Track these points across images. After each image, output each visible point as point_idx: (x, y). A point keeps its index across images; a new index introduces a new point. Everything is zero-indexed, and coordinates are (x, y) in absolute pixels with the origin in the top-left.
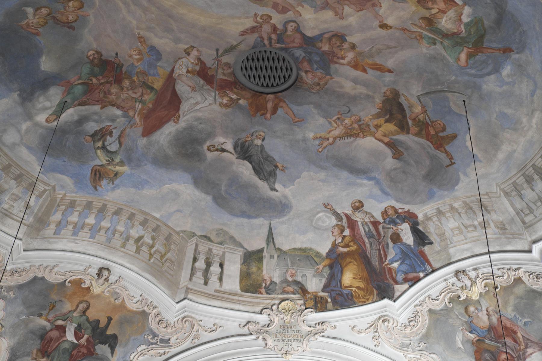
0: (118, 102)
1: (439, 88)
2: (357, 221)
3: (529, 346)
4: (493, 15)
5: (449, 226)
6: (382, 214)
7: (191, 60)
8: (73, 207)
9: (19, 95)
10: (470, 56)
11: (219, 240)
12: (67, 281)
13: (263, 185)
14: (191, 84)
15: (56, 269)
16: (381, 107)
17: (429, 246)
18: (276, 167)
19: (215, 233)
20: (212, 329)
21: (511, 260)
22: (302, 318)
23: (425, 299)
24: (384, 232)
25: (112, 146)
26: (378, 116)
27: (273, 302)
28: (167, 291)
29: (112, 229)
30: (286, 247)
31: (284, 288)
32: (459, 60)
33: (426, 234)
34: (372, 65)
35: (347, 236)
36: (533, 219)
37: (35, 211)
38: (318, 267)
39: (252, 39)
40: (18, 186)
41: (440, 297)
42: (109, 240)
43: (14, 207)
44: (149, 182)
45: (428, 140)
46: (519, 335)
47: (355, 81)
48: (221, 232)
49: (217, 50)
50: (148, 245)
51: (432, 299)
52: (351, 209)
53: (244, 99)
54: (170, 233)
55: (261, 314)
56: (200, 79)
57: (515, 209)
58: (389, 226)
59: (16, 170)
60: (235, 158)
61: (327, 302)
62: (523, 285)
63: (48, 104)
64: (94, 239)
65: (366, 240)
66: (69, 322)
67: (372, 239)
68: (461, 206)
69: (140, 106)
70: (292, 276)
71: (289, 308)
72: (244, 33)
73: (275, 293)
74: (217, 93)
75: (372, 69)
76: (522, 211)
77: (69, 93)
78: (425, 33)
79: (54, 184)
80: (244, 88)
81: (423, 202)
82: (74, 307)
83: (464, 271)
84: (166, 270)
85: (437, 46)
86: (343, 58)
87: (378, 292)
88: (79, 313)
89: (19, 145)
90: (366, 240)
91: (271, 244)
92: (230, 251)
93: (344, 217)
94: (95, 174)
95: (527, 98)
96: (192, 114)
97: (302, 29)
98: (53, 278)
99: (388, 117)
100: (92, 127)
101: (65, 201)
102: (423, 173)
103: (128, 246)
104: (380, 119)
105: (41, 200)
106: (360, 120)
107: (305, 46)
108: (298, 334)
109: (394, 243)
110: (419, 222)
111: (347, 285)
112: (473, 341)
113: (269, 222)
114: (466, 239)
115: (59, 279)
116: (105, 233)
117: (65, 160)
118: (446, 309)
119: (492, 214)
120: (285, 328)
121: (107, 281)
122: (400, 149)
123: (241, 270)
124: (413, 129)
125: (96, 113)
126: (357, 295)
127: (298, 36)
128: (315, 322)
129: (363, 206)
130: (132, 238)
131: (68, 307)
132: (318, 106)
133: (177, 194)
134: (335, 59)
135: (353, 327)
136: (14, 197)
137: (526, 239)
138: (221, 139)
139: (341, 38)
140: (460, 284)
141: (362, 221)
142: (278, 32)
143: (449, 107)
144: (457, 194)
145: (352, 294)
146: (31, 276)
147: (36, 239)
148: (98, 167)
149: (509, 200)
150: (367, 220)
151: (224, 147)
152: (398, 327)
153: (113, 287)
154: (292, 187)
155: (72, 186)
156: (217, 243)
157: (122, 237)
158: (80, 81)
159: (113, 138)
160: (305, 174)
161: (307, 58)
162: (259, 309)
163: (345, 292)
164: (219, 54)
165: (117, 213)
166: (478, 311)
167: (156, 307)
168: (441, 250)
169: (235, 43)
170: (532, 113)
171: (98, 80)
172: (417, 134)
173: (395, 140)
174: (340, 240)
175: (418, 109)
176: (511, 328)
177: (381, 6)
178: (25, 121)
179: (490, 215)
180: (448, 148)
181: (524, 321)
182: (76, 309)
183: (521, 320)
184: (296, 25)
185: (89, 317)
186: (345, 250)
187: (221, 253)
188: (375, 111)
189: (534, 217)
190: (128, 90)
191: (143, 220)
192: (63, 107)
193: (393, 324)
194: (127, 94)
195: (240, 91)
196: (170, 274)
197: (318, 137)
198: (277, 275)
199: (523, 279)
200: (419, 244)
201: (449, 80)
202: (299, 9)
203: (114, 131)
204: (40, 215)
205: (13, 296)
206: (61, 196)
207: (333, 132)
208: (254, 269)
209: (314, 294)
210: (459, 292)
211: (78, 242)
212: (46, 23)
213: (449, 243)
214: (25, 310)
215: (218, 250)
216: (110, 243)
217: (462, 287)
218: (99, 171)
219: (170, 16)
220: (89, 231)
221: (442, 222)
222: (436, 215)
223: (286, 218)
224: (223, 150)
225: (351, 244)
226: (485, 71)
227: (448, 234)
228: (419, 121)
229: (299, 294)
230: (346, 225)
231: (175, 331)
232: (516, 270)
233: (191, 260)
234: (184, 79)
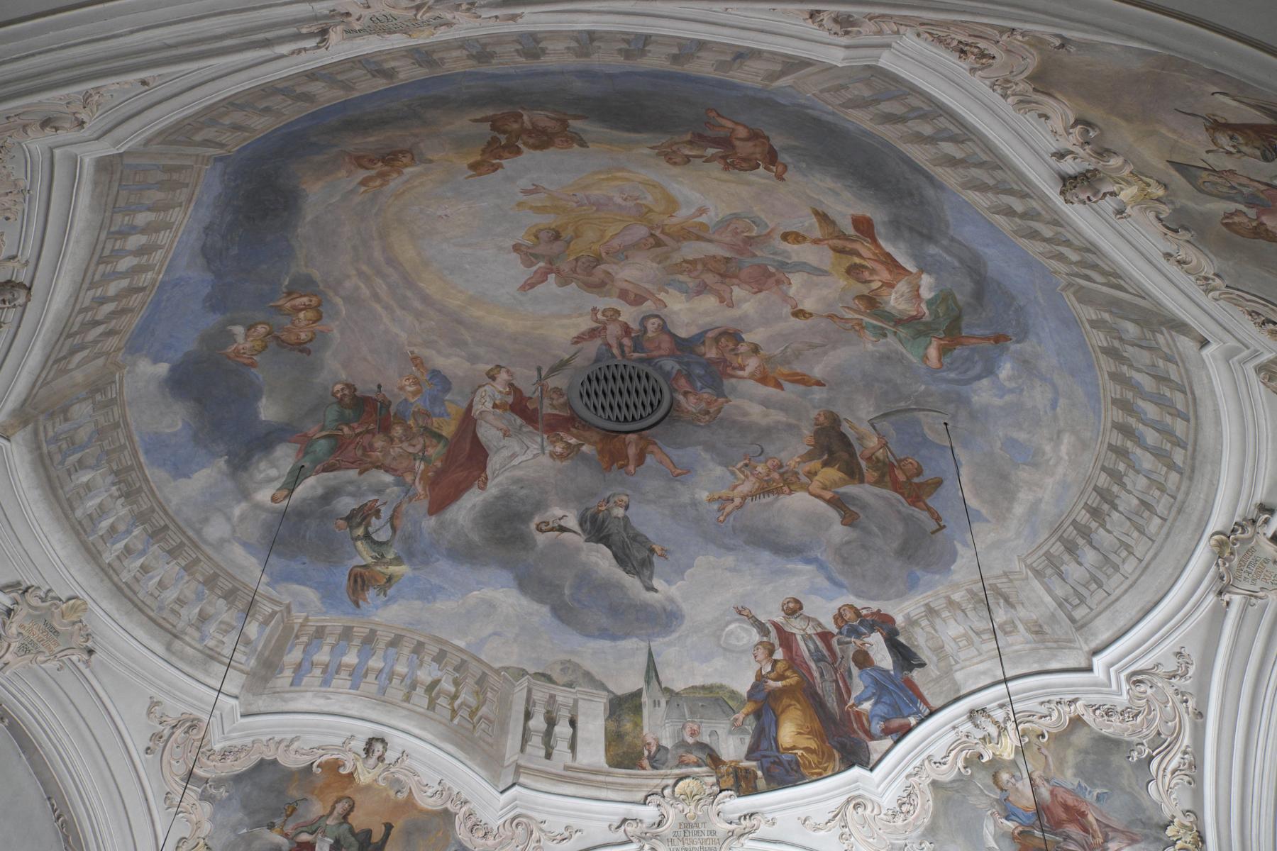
0: (388, 461)
1: (902, 404)
2: (795, 634)
3: (1110, 837)
4: (969, 286)
5: (950, 634)
6: (835, 619)
7: (500, 385)
8: (322, 638)
9: (228, 462)
10: (943, 351)
11: (566, 679)
12: (315, 765)
13: (632, 583)
14: (501, 426)
15: (295, 745)
16: (813, 443)
17: (919, 669)
18: (652, 551)
19: (558, 668)
20: (563, 837)
21: (1061, 686)
22: (715, 808)
23: (922, 764)
24: (840, 649)
25: (381, 533)
26: (809, 457)
27: (665, 782)
28: (483, 773)
29: (386, 670)
30: (678, 686)
31: (681, 756)
32: (927, 358)
33: (913, 649)
34: (788, 375)
35: (779, 661)
36: (1087, 614)
37: (259, 649)
38: (736, 716)
39: (592, 347)
40: (230, 608)
41: (948, 758)
42: (383, 690)
43: (224, 643)
44: (444, 588)
45: (896, 491)
46: (1091, 818)
47: (766, 403)
48: (567, 666)
49: (539, 370)
50: (447, 694)
51: (935, 763)
52: (783, 614)
53: (590, 443)
54: (484, 673)
55: (645, 804)
56: (516, 417)
57: (1055, 598)
58: (848, 639)
59: (227, 583)
60: (582, 540)
61: (756, 777)
62: (1085, 730)
63: (273, 472)
64: (357, 689)
65: (813, 665)
66: (320, 836)
67: (823, 663)
68: (965, 598)
69: (422, 467)
70: (693, 734)
71: (692, 792)
72: (578, 340)
73: (667, 767)
74: (545, 436)
75: (793, 382)
76: (1066, 600)
77: (306, 454)
78: (867, 319)
79: (288, 602)
80: (587, 426)
81: (901, 595)
82: (329, 809)
83: (983, 710)
84: (480, 738)
85: (888, 340)
86: (742, 368)
87: (842, 755)
88: (337, 819)
89: (229, 541)
90: (813, 665)
91: (654, 681)
92: (586, 698)
93: (771, 628)
94: (356, 581)
95: (1046, 412)
96: (507, 474)
97: (669, 326)
98: (292, 761)
99: (826, 457)
100: (346, 504)
101: (307, 628)
102: (895, 545)
103: (415, 699)
104: (813, 463)
105: (268, 630)
106: (781, 466)
107: (678, 353)
108: (710, 837)
109: (860, 668)
110: (899, 628)
111: (788, 746)
112: (1013, 833)
113: (647, 644)
114: (980, 654)
115: (303, 761)
116: (376, 678)
117: (306, 560)
118: (960, 779)
119: (1018, 608)
120: (687, 827)
121: (383, 761)
122: (852, 508)
123: (606, 729)
124: (870, 475)
125: (351, 482)
126: (807, 762)
127: (665, 338)
128: (737, 815)
129: (801, 608)
130: (421, 684)
131: (317, 808)
132: (710, 447)
133: (491, 605)
134: (729, 371)
135: (805, 820)
136: (223, 627)
137: (1081, 649)
138: (558, 512)
139: (735, 336)
140: (979, 734)
141: (802, 633)
142: (633, 335)
143: (924, 436)
144: (956, 577)
145: (797, 762)
146: (255, 759)
148: (359, 569)
149: (1043, 583)
150: (810, 631)
151: (563, 523)
152: (882, 816)
153: (392, 770)
154: (680, 583)
155: (319, 604)
156: (564, 685)
157: (403, 684)
158: (324, 433)
159: (381, 520)
160: (700, 560)
161: (684, 372)
162: (640, 796)
163: (784, 757)
164: (543, 375)
165: (395, 643)
166: (1016, 781)
167: (466, 802)
168: (940, 677)
169: (567, 357)
170: (1058, 437)
171: (352, 429)
172: (879, 483)
173: (845, 494)
174: (769, 669)
175: (873, 442)
176: (1075, 806)
177: (790, 284)
178: (239, 502)
179: (1016, 610)
180: (930, 502)
181: (1095, 794)
182: (331, 813)
183: (1090, 792)
184: (661, 323)
185: (354, 825)
186: (780, 684)
187: (571, 701)
188: (804, 449)
189: (1089, 610)
190: (401, 441)
191: (438, 653)
192: (298, 475)
193: (873, 811)
194: (401, 448)
195: (582, 432)
196: (488, 743)
197: (716, 497)
198: (668, 735)
199: (1085, 718)
200: (903, 669)
201: (917, 391)
202: (662, 296)
203: (383, 509)
204: (267, 654)
205: (225, 795)
206: (300, 621)
207: (739, 489)
208: (628, 726)
209: (733, 764)
210: (980, 748)
211: (331, 696)
212: (266, 347)
213: (953, 663)
214: (246, 818)
215: (564, 697)
216: (384, 694)
217: (984, 738)
218: (361, 576)
219: (460, 322)
220: (350, 676)
221: (937, 627)
222: (926, 615)
223: (675, 635)
224: (563, 529)
225: (788, 673)
226: (971, 373)
227: (950, 647)
228: (878, 460)
229: (707, 765)
230: (776, 642)
231: (501, 843)
232: (1071, 702)
233: (522, 716)
234: (490, 418)
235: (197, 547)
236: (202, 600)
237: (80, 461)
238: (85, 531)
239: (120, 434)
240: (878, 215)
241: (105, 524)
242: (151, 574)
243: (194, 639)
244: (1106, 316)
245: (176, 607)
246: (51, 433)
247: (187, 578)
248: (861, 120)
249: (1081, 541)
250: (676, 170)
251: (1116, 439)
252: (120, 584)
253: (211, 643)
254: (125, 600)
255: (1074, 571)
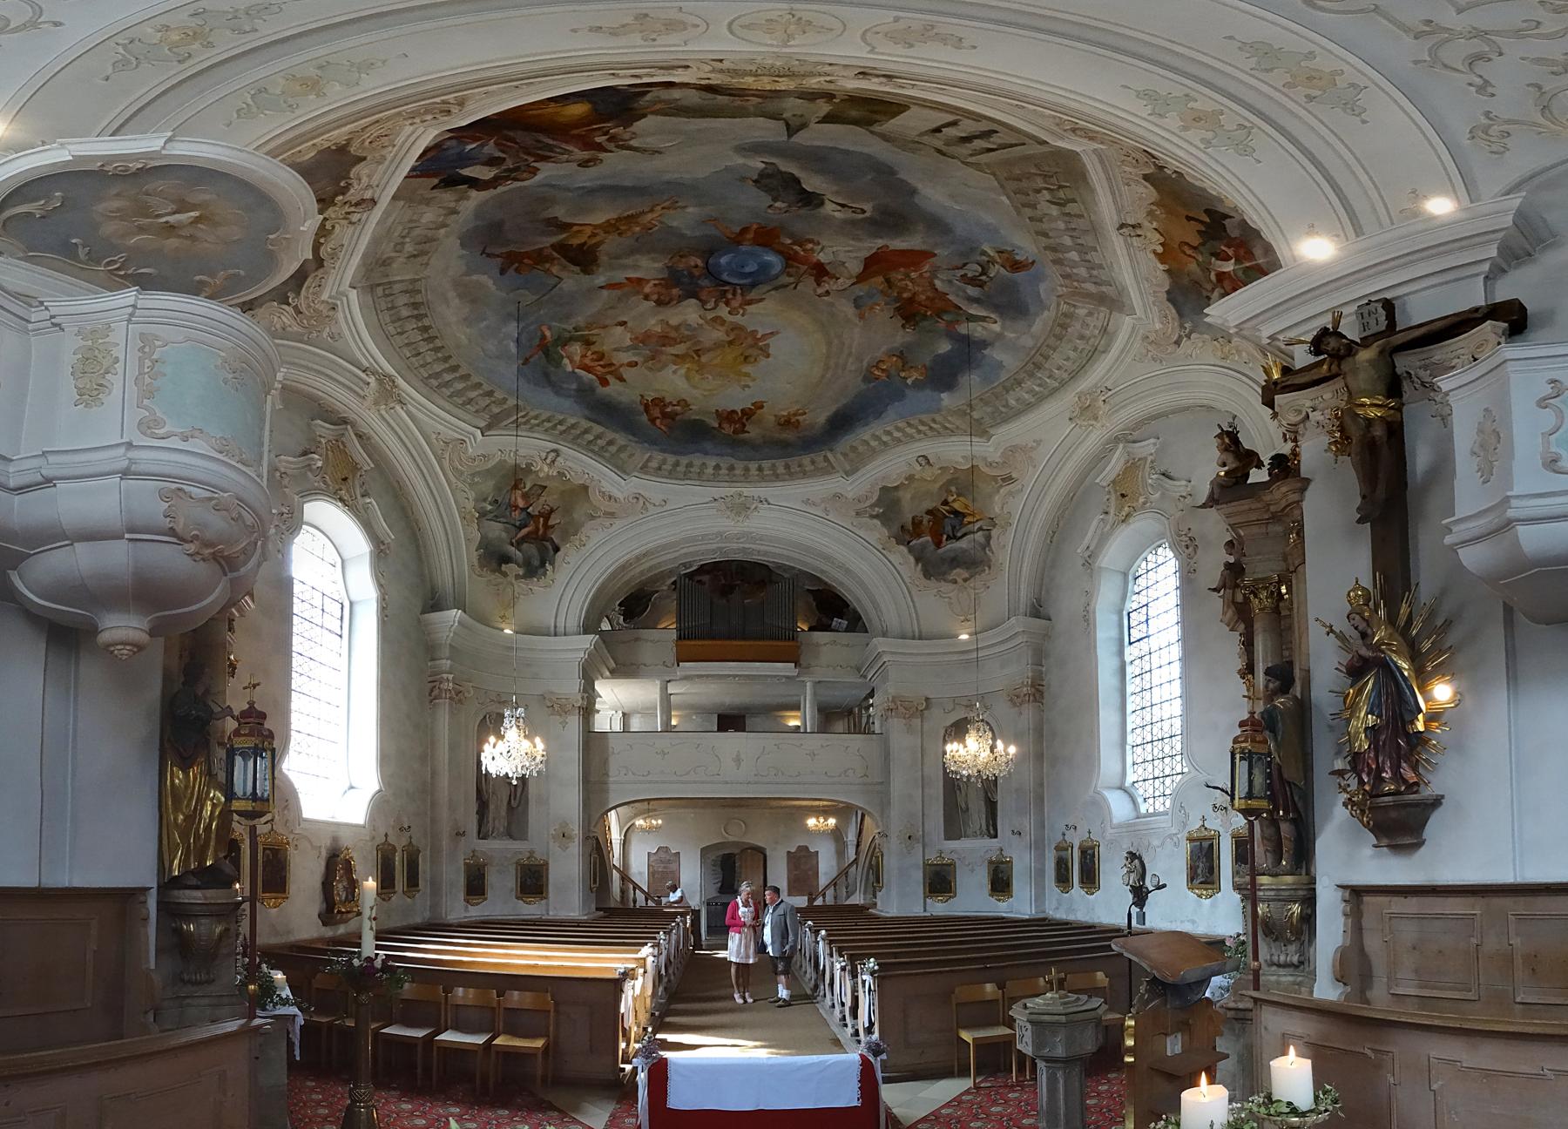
57: (395, 282)
240: (602, 391)
244: (505, 407)
248: (621, 439)
249: (416, 312)
250: (684, 396)
251: (452, 362)
255: (402, 300)
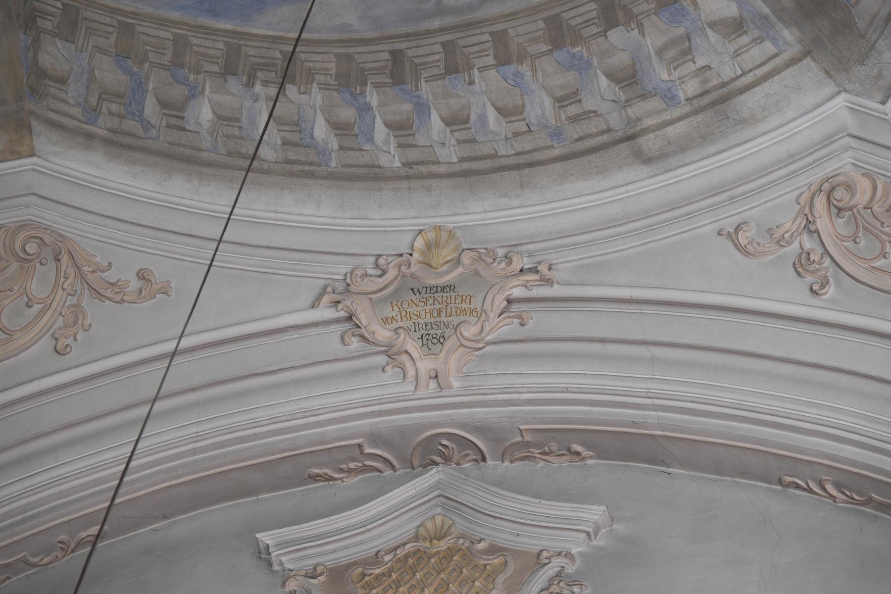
37: (766, 10)
40: (640, 26)
43: (708, 68)
136: (671, 53)
147: (872, 47)
235: (470, 25)
236: (589, 63)
237: (163, 104)
238: (312, 163)
239: (147, 30)
241: (321, 131)
242: (473, 117)
243: (658, 112)
245: (573, 110)
246: (75, 111)
247: (525, 69)
252: (457, 168)
253: (692, 87)
254: (495, 177)
